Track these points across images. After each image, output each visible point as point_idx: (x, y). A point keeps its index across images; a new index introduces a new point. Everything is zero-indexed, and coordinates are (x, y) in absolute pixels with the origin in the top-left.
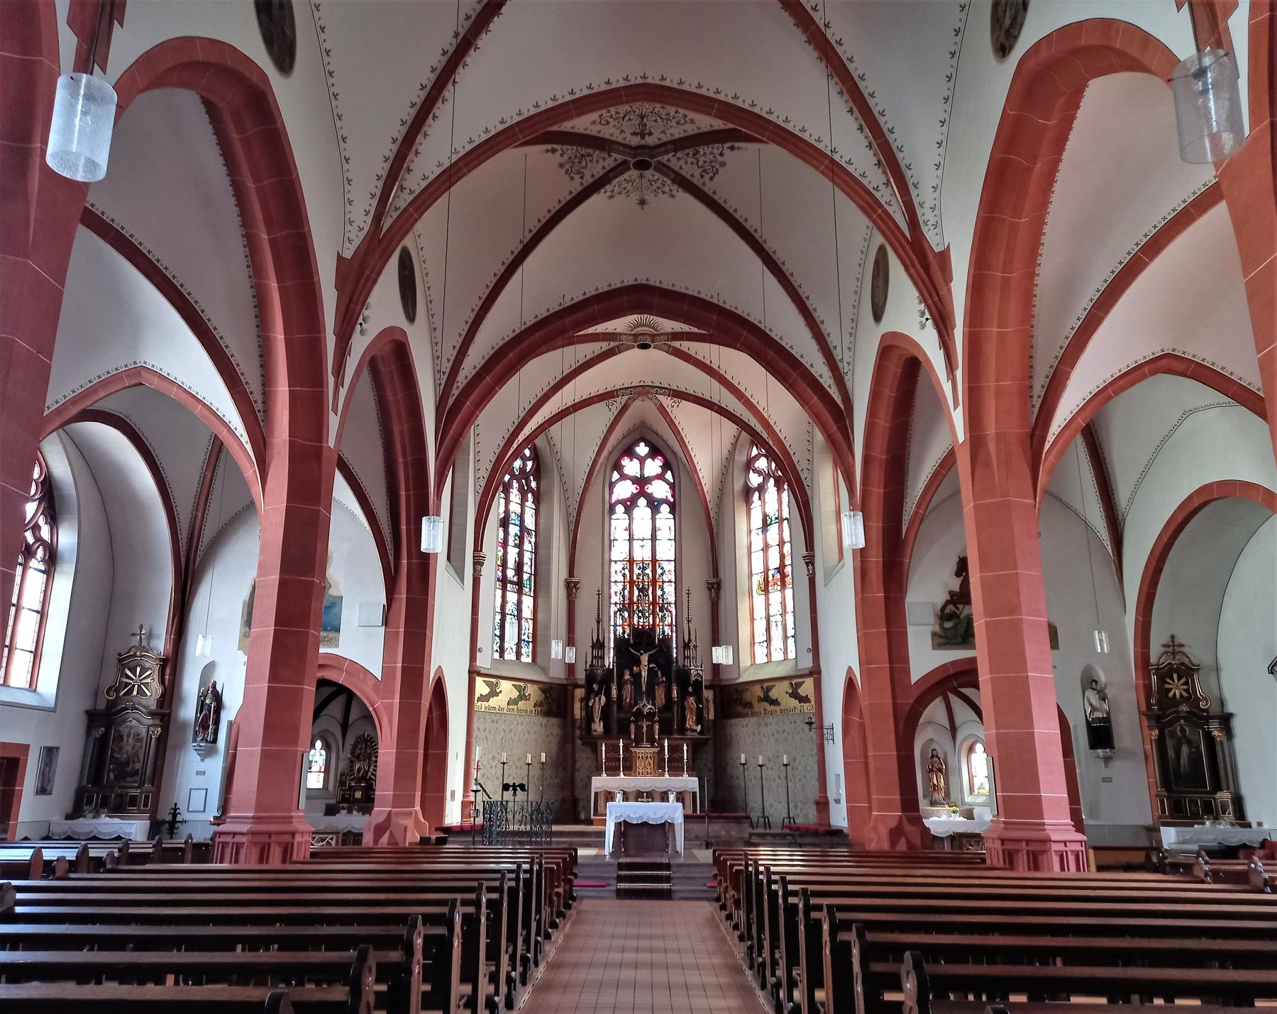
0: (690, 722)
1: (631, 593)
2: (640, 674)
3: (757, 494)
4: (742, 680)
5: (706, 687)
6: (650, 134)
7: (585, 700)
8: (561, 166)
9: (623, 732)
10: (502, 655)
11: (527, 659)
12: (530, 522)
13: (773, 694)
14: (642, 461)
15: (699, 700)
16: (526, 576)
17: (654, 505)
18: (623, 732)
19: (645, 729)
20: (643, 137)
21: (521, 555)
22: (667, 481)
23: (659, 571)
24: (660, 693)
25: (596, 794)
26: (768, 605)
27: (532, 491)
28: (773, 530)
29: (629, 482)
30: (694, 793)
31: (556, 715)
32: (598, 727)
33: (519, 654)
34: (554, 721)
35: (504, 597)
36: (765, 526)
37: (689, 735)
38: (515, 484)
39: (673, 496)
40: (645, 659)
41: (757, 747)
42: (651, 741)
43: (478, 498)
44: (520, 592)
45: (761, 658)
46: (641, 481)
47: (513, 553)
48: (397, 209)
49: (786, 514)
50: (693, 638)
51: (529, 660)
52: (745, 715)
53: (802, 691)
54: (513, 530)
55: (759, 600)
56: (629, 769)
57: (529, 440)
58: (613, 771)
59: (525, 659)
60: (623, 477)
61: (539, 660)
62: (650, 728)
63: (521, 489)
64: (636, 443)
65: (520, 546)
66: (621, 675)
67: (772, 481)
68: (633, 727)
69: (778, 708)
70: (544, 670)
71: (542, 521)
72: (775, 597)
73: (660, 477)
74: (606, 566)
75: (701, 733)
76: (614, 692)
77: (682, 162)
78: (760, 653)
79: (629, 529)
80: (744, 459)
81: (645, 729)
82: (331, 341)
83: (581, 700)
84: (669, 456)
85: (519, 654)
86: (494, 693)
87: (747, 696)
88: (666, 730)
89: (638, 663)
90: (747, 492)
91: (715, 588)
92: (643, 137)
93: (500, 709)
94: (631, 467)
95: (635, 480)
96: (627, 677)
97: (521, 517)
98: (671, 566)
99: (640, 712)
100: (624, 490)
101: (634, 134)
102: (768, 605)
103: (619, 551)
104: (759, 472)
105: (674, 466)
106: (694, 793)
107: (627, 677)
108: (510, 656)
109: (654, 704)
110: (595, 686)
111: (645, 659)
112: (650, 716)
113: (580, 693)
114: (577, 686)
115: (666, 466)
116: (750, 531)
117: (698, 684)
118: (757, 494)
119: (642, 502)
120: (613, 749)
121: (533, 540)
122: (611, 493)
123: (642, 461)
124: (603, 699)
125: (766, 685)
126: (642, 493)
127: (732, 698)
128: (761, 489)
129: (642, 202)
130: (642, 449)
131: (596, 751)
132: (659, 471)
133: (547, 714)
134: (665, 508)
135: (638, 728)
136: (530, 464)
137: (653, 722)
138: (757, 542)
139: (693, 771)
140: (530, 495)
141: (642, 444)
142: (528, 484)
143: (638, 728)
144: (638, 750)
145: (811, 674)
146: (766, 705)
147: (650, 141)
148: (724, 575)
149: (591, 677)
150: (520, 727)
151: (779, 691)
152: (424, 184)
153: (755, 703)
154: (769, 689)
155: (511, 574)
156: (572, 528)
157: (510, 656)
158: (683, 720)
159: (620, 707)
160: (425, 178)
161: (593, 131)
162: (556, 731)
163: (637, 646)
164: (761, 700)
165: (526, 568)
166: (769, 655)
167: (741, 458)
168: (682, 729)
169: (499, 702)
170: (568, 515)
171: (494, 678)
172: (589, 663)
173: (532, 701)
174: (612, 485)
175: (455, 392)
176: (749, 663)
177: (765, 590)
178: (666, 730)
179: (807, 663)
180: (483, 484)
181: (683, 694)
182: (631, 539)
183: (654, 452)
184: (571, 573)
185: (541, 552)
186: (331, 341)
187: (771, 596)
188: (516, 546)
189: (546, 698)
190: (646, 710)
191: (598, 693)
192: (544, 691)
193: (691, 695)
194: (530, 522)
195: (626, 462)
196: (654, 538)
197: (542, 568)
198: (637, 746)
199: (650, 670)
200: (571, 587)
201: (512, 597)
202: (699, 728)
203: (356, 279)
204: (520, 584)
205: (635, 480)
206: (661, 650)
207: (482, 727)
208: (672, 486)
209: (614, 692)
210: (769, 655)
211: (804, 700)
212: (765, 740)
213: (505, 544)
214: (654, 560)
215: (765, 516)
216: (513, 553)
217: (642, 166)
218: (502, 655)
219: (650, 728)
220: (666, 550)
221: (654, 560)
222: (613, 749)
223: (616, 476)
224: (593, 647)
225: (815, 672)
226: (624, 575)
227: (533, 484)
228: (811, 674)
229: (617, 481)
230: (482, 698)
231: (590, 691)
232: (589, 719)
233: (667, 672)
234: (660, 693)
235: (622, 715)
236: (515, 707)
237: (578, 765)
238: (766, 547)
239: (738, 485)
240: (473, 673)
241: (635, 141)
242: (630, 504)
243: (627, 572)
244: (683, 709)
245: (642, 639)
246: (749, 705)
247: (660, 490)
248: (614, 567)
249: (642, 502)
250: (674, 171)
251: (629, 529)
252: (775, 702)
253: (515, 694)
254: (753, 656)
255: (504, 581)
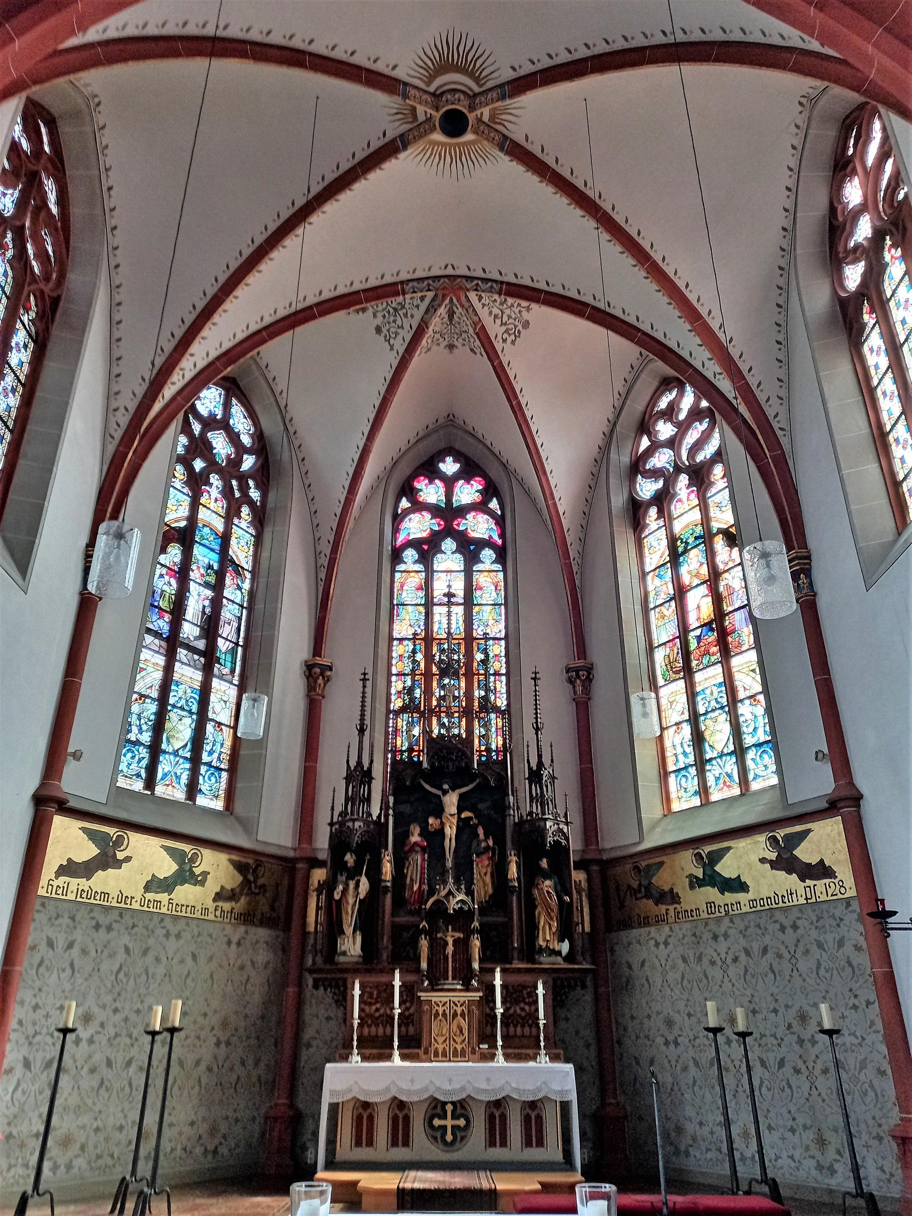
0: (547, 934)
1: (428, 692)
2: (440, 833)
3: (653, 512)
4: (647, 844)
5: (579, 866)
7: (328, 887)
9: (404, 956)
10: (150, 783)
11: (211, 799)
12: (241, 550)
13: (727, 868)
14: (449, 483)
15: (563, 887)
16: (222, 645)
17: (470, 549)
18: (404, 956)
19: (450, 949)
21: (217, 603)
22: (491, 513)
23: (479, 656)
24: (482, 871)
25: (334, 1109)
26: (692, 695)
27: (251, 503)
28: (694, 564)
29: (427, 516)
30: (565, 1107)
31: (266, 922)
32: (351, 946)
33: (192, 789)
34: (262, 933)
35: (168, 670)
36: (675, 557)
37: (546, 961)
38: (215, 479)
39: (502, 535)
40: (451, 801)
41: (681, 989)
42: (465, 976)
43: (111, 448)
44: (208, 671)
45: (683, 797)
46: (448, 513)
47: (197, 600)
49: (723, 518)
50: (546, 760)
51: (219, 805)
52: (660, 920)
53: (805, 853)
54: (204, 556)
55: (673, 693)
56: (414, 1045)
57: (233, 374)
58: (376, 1048)
59: (201, 801)
60: (418, 506)
61: (238, 807)
62: (463, 946)
63: (227, 492)
64: (440, 455)
65: (218, 587)
66: (402, 836)
67: (684, 479)
68: (424, 943)
69: (741, 897)
70: (247, 826)
71: (265, 554)
72: (709, 678)
73: (481, 507)
74: (383, 644)
75: (570, 958)
76: (387, 868)
78: (683, 797)
79: (427, 587)
80: (626, 459)
81: (450, 949)
83: (319, 891)
84: (495, 472)
85: (192, 789)
86: (107, 859)
87: (662, 880)
88: (496, 952)
89: (439, 811)
90: (636, 511)
91: (581, 676)
93: (123, 898)
94: (431, 492)
95: (435, 511)
96: (415, 838)
97: (225, 539)
98: (498, 649)
99: (440, 906)
100: (418, 526)
102: (692, 695)
103: (407, 624)
104: (655, 474)
105: (504, 488)
106: (565, 1107)
107: (415, 838)
108: (172, 790)
109: (470, 893)
110: (349, 859)
111: (451, 801)
112: (462, 918)
113: (319, 875)
114: (315, 863)
115: (490, 490)
116: (643, 575)
117: (559, 851)
118: (653, 512)
119: (449, 544)
120: (379, 995)
121: (246, 586)
122: (396, 531)
123: (449, 483)
124: (364, 884)
125: (707, 849)
126: (448, 531)
127: (624, 891)
128: (662, 500)
130: (449, 467)
131: (343, 999)
132: (477, 497)
133: (247, 918)
134: (488, 554)
135: (437, 947)
136: (248, 462)
137: (469, 933)
138: (660, 587)
139: (560, 1050)
140: (245, 510)
141: (449, 460)
142: (244, 489)
143: (437, 947)
144: (436, 997)
145: (832, 807)
146: (711, 893)
148: (599, 654)
149: (340, 841)
150: (172, 944)
151: (746, 858)
153: (682, 888)
154: (715, 857)
155: (190, 631)
156: (322, 575)
157: (172, 790)
158: (531, 929)
159: (399, 903)
162: (263, 956)
163: (436, 775)
164: (695, 883)
165: (226, 630)
166: (703, 790)
167: (622, 458)
168: (530, 951)
169: (119, 884)
170: (317, 554)
171: (112, 823)
172: (339, 808)
173: (212, 887)
174: (398, 519)
175: (157, 407)
176: (658, 812)
177: (688, 672)
178: (496, 952)
179: (820, 782)
180: (124, 420)
181: (531, 874)
182: (429, 605)
183: (469, 470)
184: (317, 650)
185: (259, 606)
187: (698, 677)
188: (207, 585)
189: (246, 883)
190: (453, 905)
191: (354, 873)
192: (240, 868)
193: (546, 876)
194: (241, 550)
195: (421, 484)
196: (469, 602)
197: (256, 634)
198: (433, 988)
199: (463, 825)
200: (316, 674)
201: (188, 674)
202: (565, 947)
204: (209, 658)
205: (435, 511)
206: (487, 787)
207: (61, 941)
208: (500, 521)
209: (387, 868)
210: (703, 790)
211: (822, 871)
212: (716, 973)
213: (182, 574)
214: (469, 638)
215: (673, 541)
216: (197, 600)
217: (454, 124)
218: (150, 783)
219: (463, 946)
220: (491, 622)
221: (469, 638)
222: (379, 995)
223: (405, 503)
224: (349, 779)
225: (846, 803)
226: (414, 661)
227: (255, 494)
228: (832, 807)
229: (407, 512)
230: (69, 869)
231: (337, 866)
232: (334, 928)
233: (496, 829)
234: (482, 871)
235: (402, 919)
236: (164, 897)
237: (308, 1034)
238: (680, 593)
239: (619, 500)
240: (47, 803)
242: (427, 549)
243: (419, 657)
244: (531, 905)
245: (449, 759)
246: (672, 897)
247: (480, 526)
248: (398, 650)
249: (449, 544)
251: (427, 587)
252: (738, 885)
253: (167, 867)
254: (667, 799)
255: (172, 643)
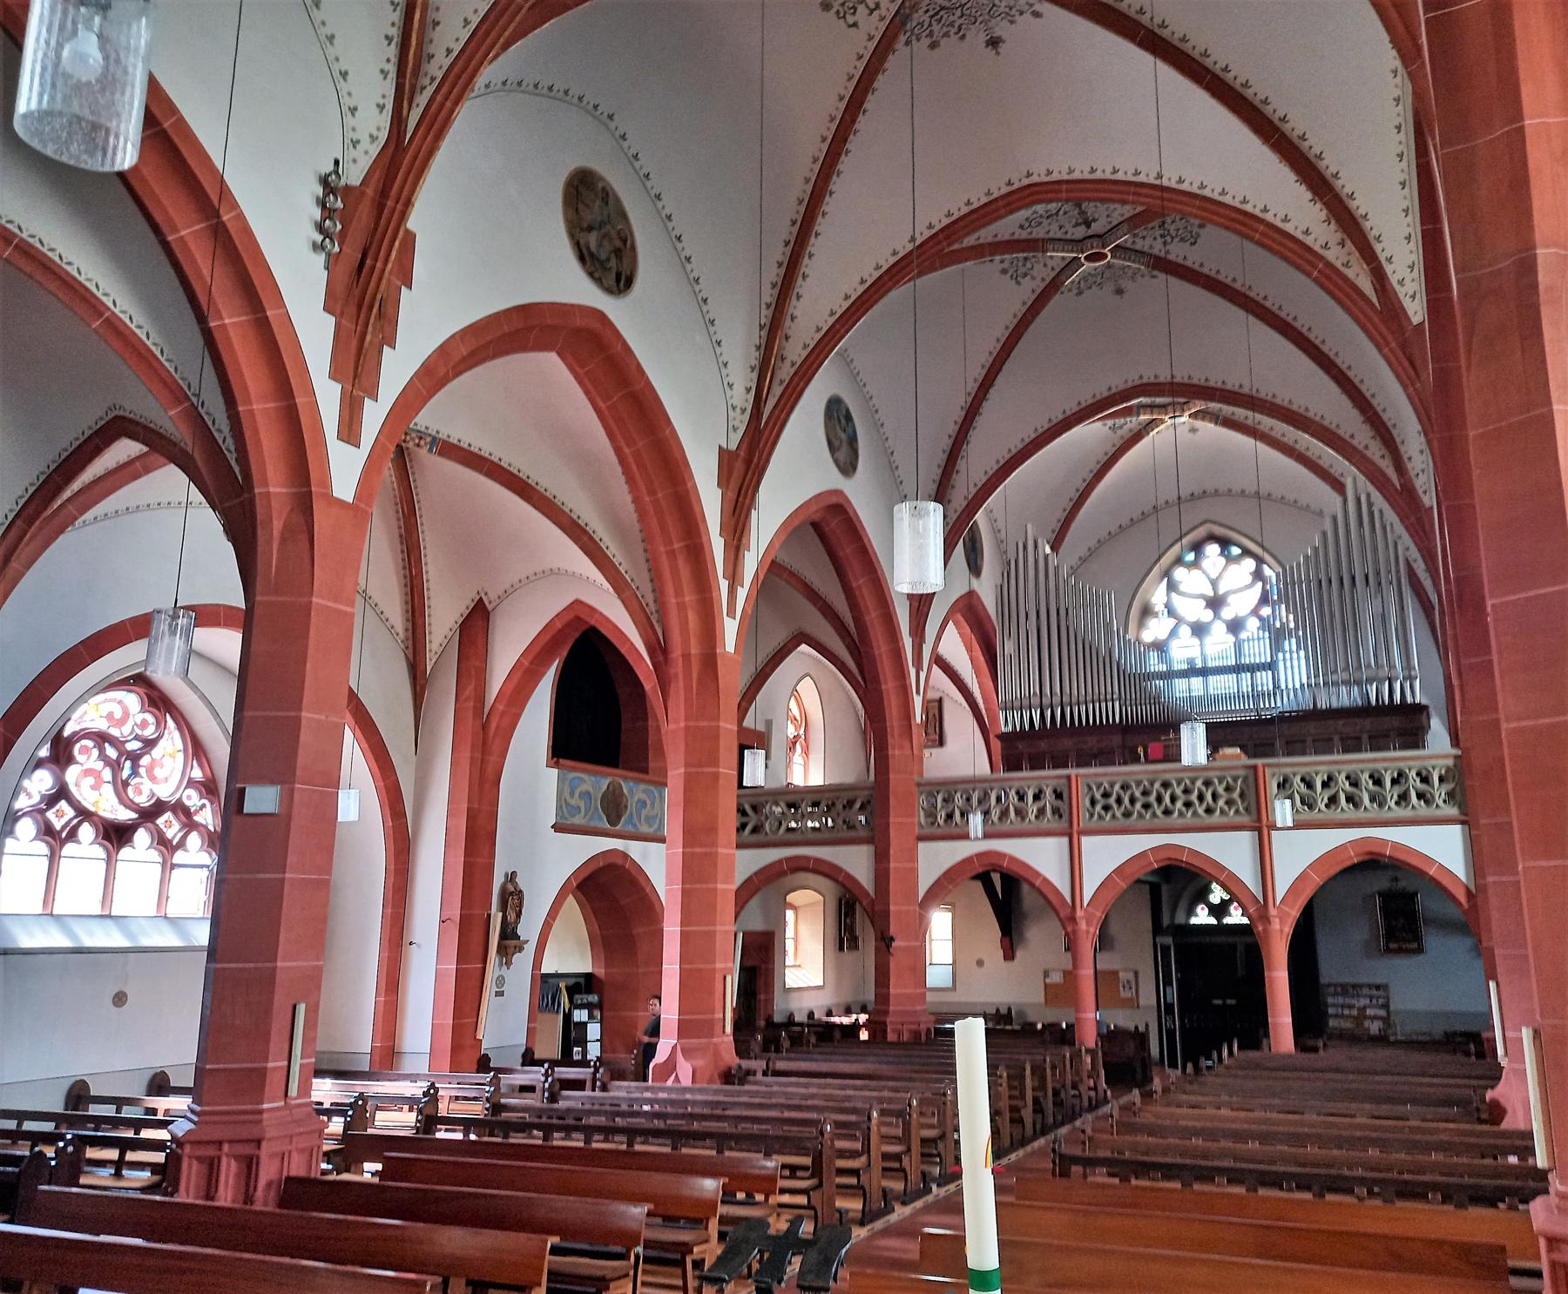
6: (1094, 220)
8: (1004, 271)
20: (1088, 224)
48: (782, 382)
77: (1149, 241)
82: (718, 545)
92: (1089, 227)
101: (1077, 224)
129: (1119, 292)
147: (1097, 228)
152: (805, 353)
160: (805, 346)
161: (1024, 235)
186: (718, 545)
203: (745, 468)
241: (1080, 232)
250: (1142, 253)
